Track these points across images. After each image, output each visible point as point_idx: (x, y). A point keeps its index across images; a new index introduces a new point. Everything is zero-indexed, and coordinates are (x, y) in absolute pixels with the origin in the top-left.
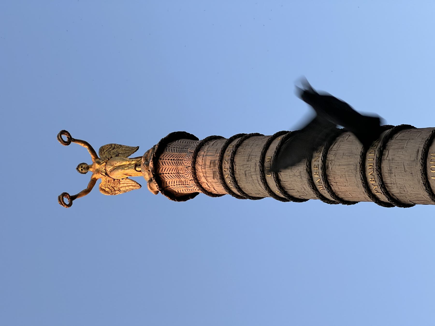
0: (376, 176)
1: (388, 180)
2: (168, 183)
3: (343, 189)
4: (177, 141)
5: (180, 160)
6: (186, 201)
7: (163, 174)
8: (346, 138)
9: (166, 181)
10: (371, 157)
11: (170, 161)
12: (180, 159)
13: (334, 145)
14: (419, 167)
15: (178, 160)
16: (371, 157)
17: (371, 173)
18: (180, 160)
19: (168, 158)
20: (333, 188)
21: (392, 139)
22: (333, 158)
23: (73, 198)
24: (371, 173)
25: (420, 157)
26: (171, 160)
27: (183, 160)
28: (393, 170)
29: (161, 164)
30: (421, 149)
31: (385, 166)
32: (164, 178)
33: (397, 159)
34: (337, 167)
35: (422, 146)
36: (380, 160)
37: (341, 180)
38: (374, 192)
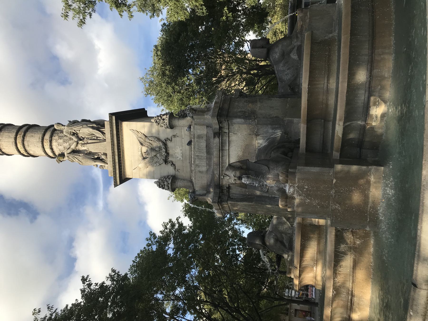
0: (22, 147)
1: (27, 149)
3: (8, 151)
10: (19, 140)
14: (40, 145)
16: (19, 140)
17: (20, 146)
20: (2, 151)
21: (27, 132)
24: (20, 146)
25: (40, 140)
28: (30, 145)
30: (41, 137)
31: (26, 143)
33: (31, 141)
34: (4, 143)
35: (41, 136)
36: (23, 141)
37: (7, 148)
38: (22, 152)
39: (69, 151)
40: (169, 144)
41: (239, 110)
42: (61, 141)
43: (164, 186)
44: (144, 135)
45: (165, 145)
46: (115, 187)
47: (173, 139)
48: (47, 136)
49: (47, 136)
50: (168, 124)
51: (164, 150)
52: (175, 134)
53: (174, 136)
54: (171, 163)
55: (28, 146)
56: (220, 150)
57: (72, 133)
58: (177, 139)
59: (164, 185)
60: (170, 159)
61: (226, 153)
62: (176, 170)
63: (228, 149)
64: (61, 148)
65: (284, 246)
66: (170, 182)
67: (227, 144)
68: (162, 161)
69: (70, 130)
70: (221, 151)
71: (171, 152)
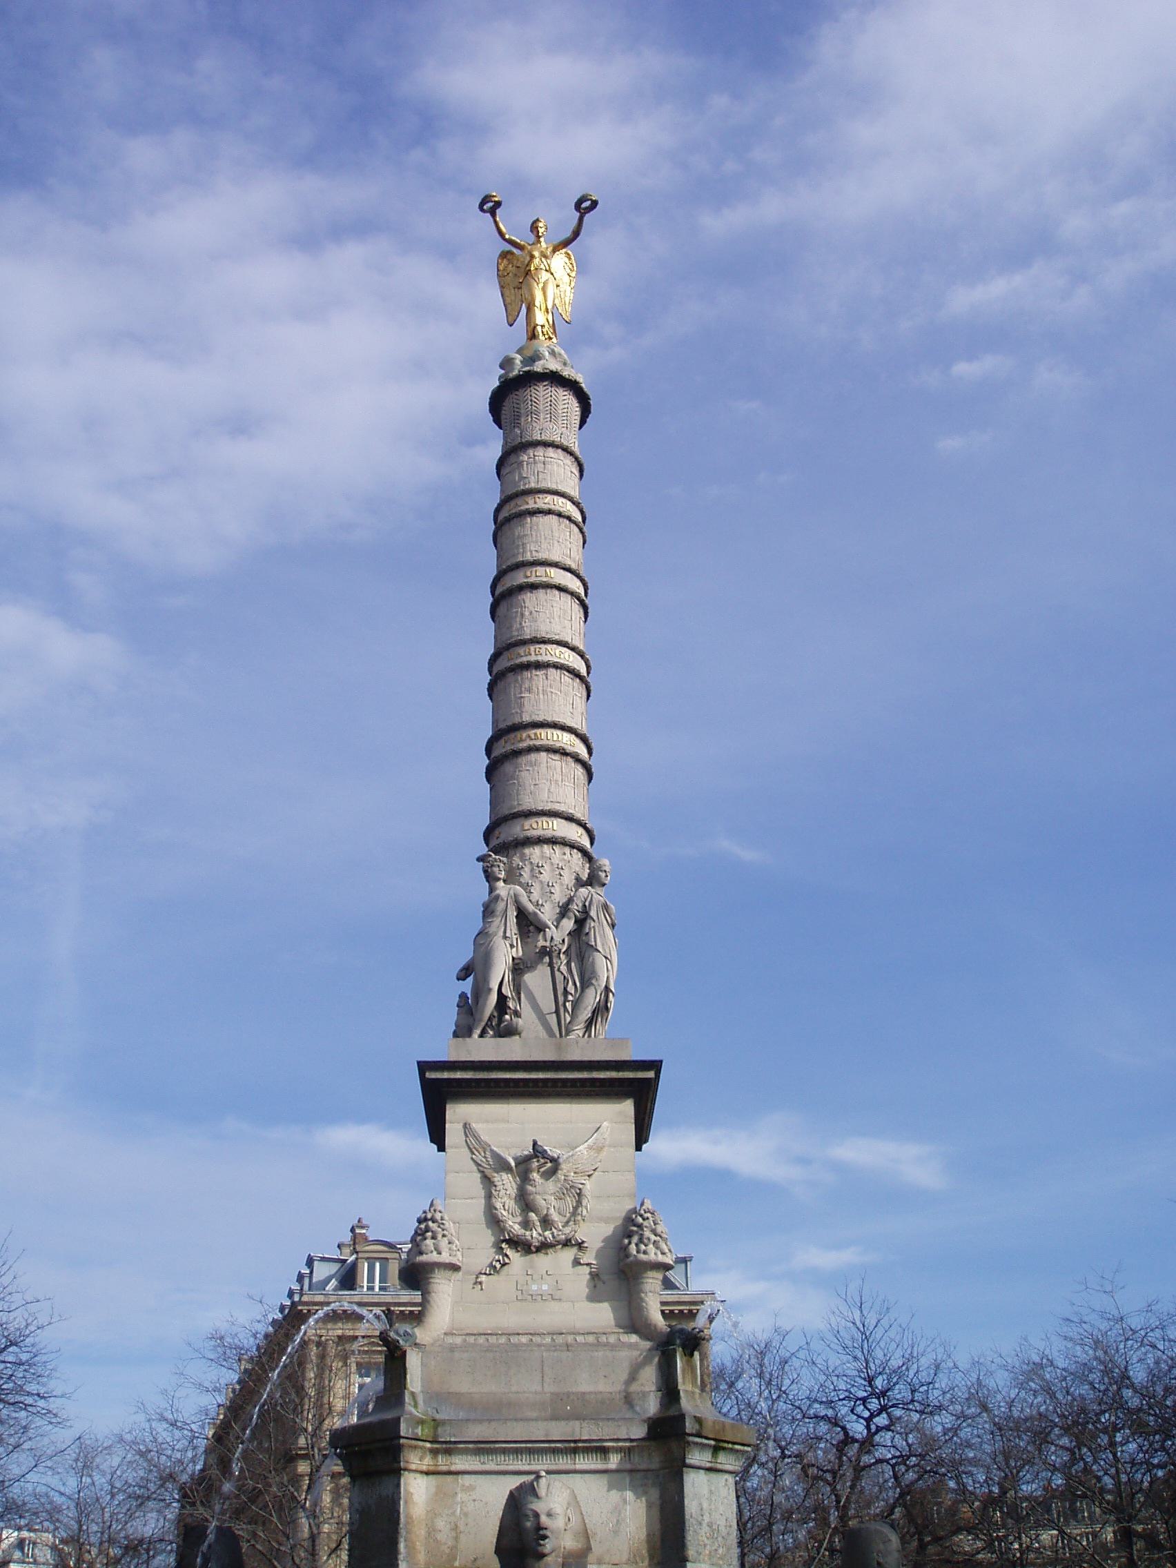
2: (517, 393)
4: (577, 405)
5: (551, 417)
6: (490, 412)
7: (530, 387)
8: (577, 694)
9: (520, 390)
11: (549, 400)
12: (553, 417)
13: (569, 677)
15: (551, 413)
18: (551, 417)
19: (553, 401)
23: (493, 214)
26: (551, 401)
27: (550, 421)
29: (545, 383)
32: (524, 387)
40: (569, 1254)
41: (705, 1505)
43: (429, 1234)
44: (594, 1170)
45: (567, 1243)
46: (423, 1067)
50: (642, 1257)
52: (604, 1277)
56: (575, 1441)
59: (434, 1238)
61: (563, 1462)
62: (483, 1278)
63: (578, 1467)
66: (445, 1257)
67: (593, 1467)
68: (514, 1225)
69: (593, 913)
70: (572, 1445)
71: (542, 1261)
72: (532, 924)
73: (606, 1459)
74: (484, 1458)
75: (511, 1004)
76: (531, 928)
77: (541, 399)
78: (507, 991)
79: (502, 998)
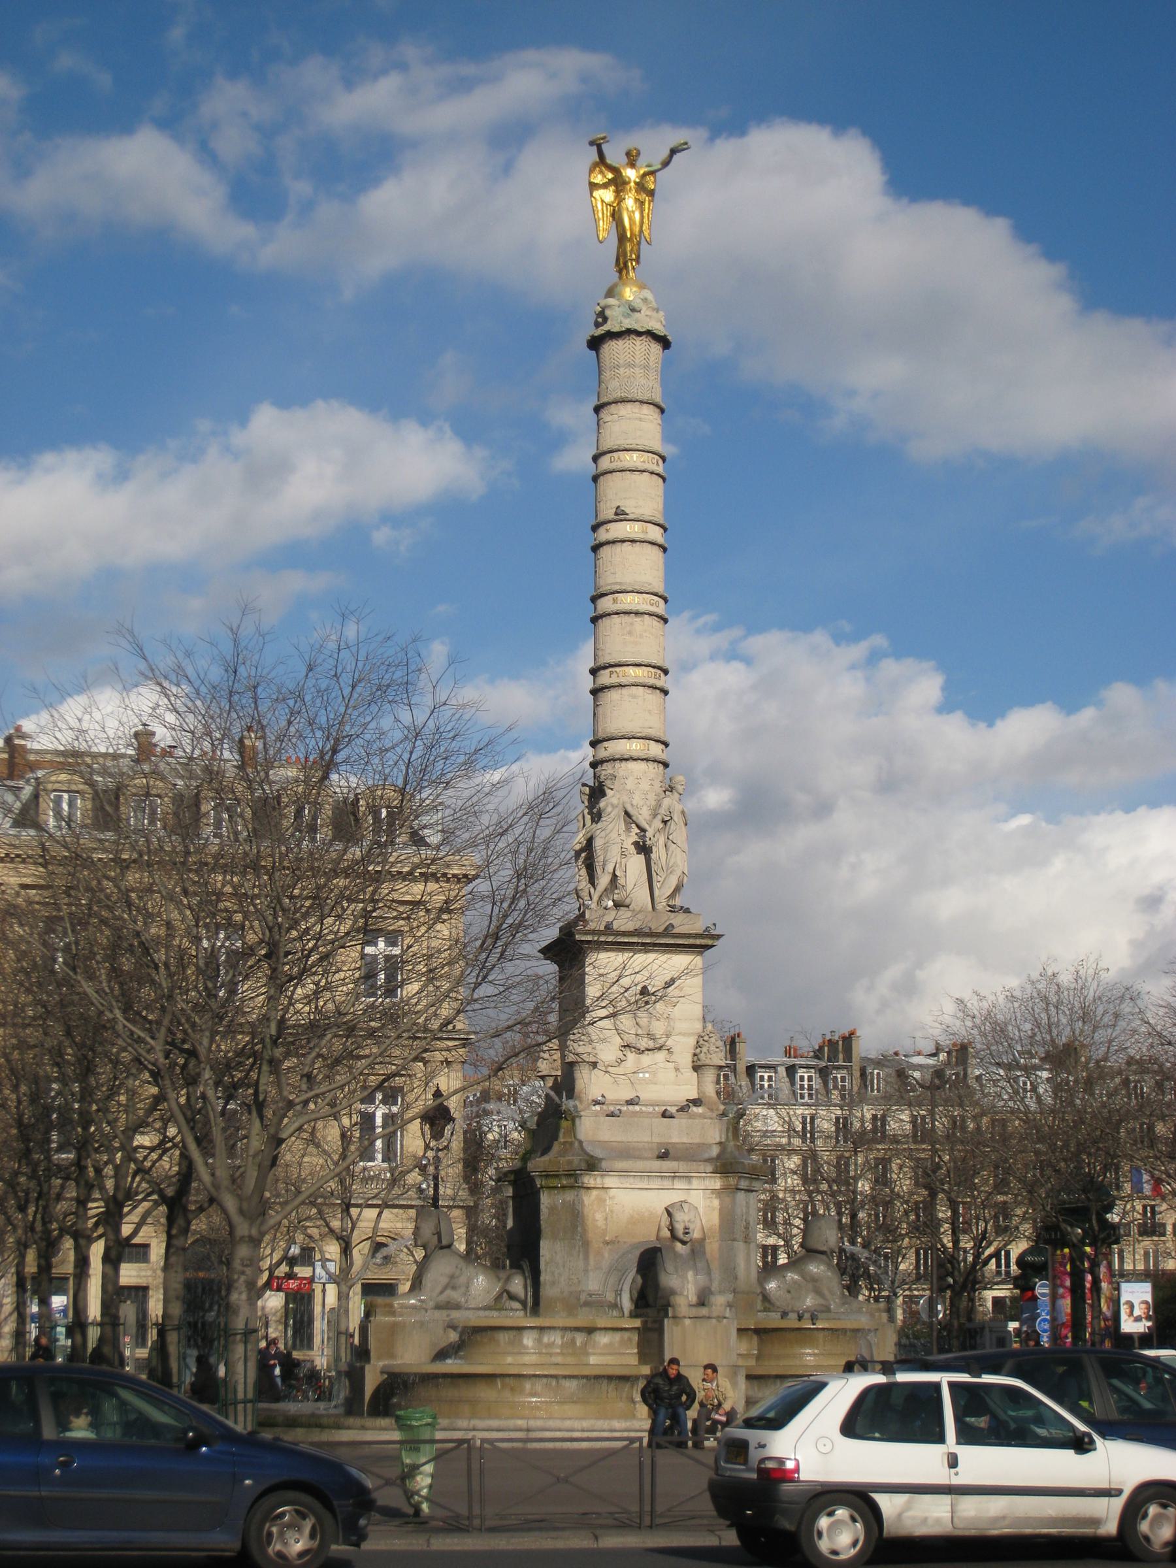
1: (625, 691)
22: (646, 623)
39: (630, 809)
40: (660, 1056)
42: (645, 785)
45: (660, 1048)
47: (671, 1065)
48: (656, 750)
49: (656, 750)
51: (651, 1044)
52: (682, 1070)
53: (677, 1070)
54: (624, 1058)
55: (634, 697)
57: (667, 818)
58: (672, 1074)
60: (631, 1056)
64: (630, 784)
65: (442, 1292)
69: (675, 818)
71: (646, 1059)
72: (634, 822)
73: (690, 1183)
74: (622, 1180)
75: (621, 881)
76: (633, 826)
77: (637, 353)
78: (618, 873)
79: (615, 877)
